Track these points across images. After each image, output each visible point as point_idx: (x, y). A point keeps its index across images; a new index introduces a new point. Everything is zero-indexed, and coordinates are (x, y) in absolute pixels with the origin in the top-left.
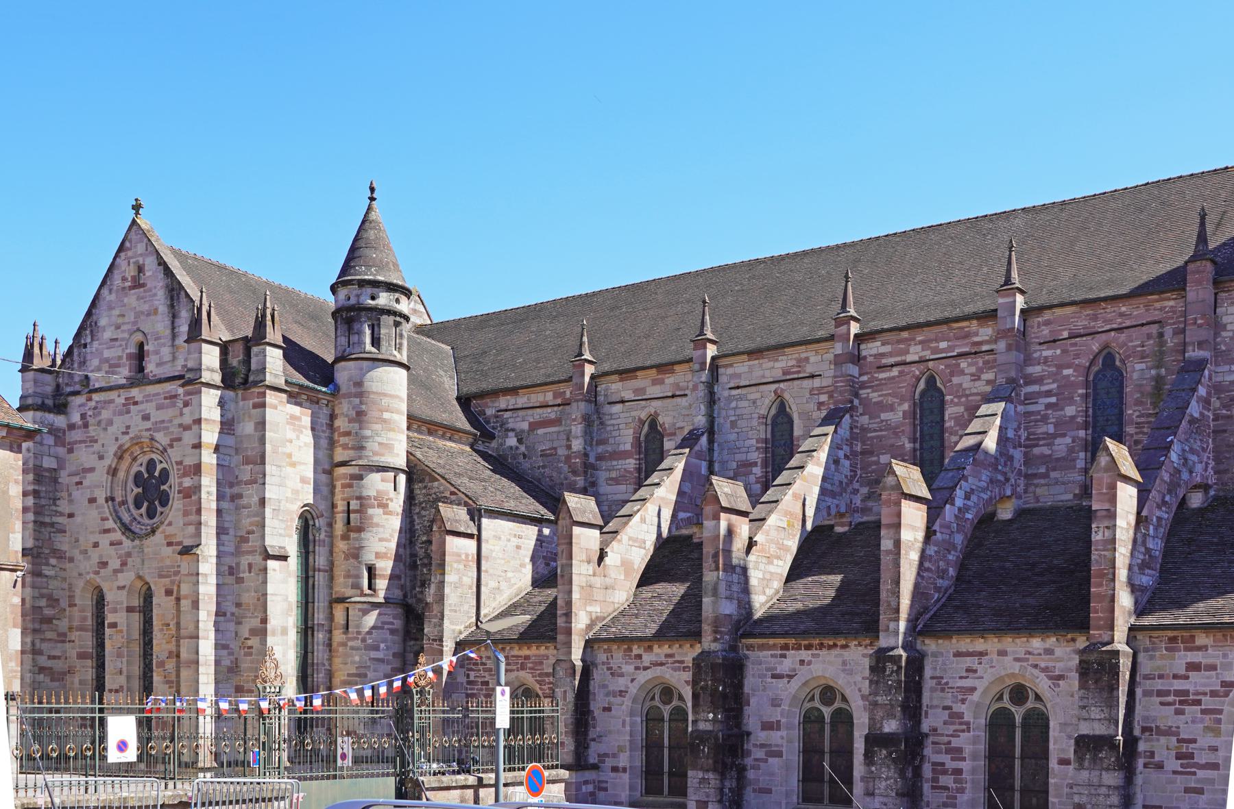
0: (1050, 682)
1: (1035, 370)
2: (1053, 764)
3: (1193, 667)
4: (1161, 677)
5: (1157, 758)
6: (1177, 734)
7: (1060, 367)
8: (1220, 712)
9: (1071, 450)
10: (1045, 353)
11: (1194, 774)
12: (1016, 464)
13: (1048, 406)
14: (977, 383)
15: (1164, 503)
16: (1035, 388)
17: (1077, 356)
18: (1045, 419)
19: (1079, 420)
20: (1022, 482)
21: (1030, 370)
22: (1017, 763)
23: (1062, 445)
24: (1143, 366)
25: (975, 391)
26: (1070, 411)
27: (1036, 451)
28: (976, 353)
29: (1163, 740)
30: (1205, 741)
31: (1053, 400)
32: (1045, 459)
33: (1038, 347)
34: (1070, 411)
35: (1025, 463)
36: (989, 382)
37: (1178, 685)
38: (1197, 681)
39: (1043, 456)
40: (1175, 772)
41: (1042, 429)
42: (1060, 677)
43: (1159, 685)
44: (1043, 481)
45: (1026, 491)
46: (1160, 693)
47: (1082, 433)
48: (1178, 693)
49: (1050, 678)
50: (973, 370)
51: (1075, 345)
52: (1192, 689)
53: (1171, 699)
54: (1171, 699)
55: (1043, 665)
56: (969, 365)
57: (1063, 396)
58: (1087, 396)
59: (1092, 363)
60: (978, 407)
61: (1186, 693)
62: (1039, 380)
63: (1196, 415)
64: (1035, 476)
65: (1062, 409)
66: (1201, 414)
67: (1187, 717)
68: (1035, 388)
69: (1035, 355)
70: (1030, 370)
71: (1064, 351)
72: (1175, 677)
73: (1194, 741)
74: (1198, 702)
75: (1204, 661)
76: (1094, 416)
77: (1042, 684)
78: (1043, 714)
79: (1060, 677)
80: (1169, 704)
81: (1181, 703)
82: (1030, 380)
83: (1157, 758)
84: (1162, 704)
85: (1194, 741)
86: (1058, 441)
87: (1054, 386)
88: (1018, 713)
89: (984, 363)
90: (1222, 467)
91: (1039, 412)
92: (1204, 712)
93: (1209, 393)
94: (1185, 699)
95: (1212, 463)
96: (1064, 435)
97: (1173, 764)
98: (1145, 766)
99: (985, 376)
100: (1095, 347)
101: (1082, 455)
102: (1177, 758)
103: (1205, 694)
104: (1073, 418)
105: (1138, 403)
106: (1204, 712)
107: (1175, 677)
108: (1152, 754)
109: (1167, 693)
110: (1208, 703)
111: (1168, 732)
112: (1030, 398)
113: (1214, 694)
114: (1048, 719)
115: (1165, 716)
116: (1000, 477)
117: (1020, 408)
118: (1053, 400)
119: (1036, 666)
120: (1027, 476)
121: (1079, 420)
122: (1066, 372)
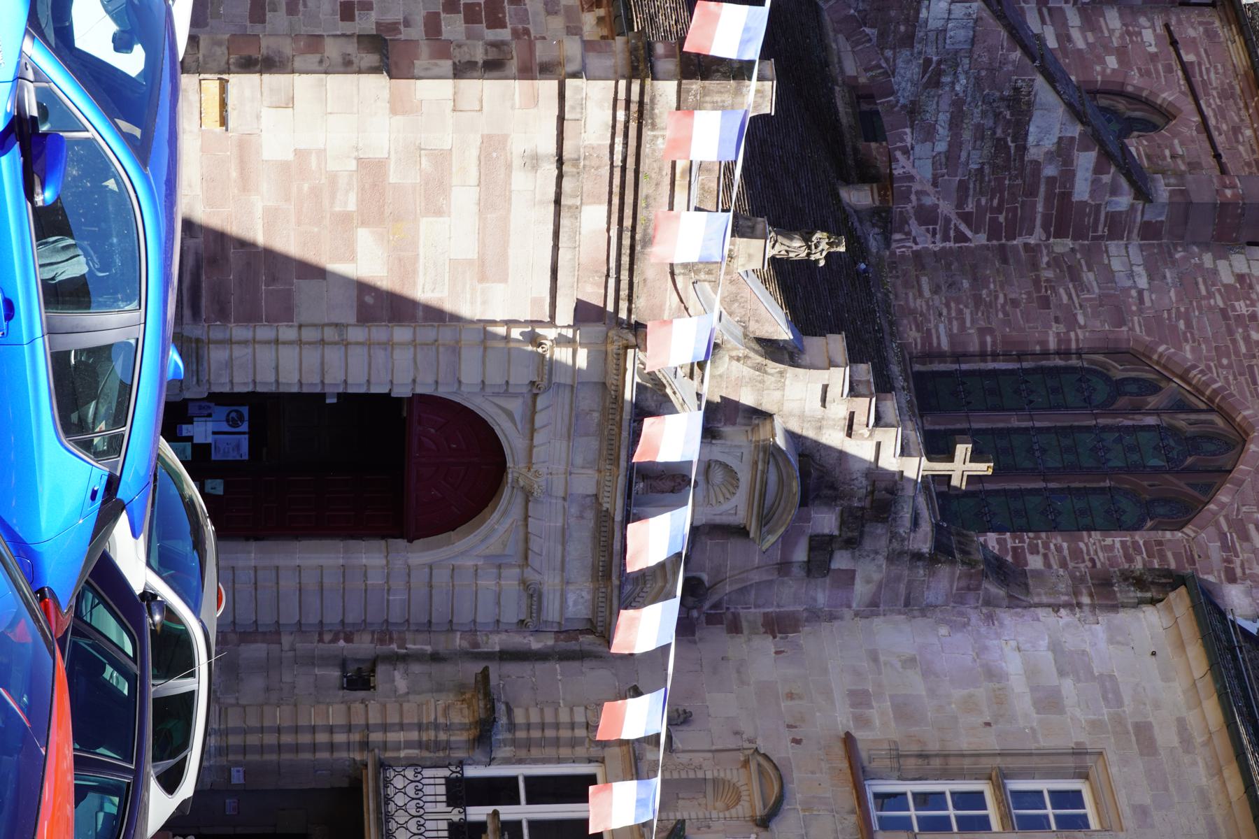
7: (1121, 53)
59: (1135, 98)
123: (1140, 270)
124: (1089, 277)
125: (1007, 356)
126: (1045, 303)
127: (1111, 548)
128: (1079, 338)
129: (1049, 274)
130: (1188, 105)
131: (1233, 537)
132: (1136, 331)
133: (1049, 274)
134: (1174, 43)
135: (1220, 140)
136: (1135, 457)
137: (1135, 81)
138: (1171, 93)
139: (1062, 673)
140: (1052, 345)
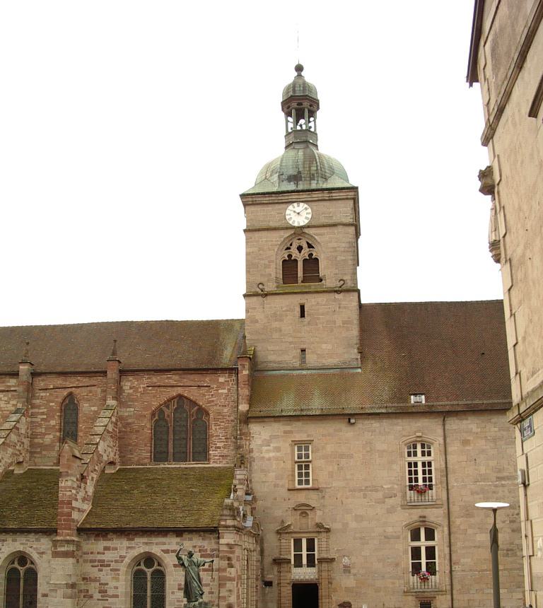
0: (38, 556)
1: (37, 402)
2: (39, 596)
3: (106, 548)
4: (92, 553)
5: (90, 593)
6: (99, 581)
8: (118, 570)
9: (53, 441)
10: (42, 394)
11: (107, 600)
12: (26, 447)
13: (42, 419)
14: (8, 405)
15: (95, 470)
16: (36, 410)
17: (57, 397)
18: (40, 425)
19: (57, 427)
20: (28, 455)
21: (34, 401)
22: (21, 597)
23: (48, 439)
24: (87, 405)
25: (6, 409)
26: (53, 423)
27: (36, 441)
28: (7, 391)
29: (93, 584)
30: (112, 584)
31: (45, 417)
32: (40, 445)
33: (37, 391)
34: (53, 423)
35: (30, 446)
36: (13, 405)
37: (99, 557)
38: (108, 556)
39: (39, 443)
40: (98, 600)
41: (39, 430)
42: (43, 553)
43: (91, 557)
44: (38, 456)
45: (30, 460)
46: (92, 561)
47: (58, 434)
48: (99, 561)
49: (38, 553)
50: (6, 399)
51: (56, 392)
52: (106, 559)
53: (96, 564)
54: (96, 564)
55: (35, 546)
56: (4, 396)
57: (50, 416)
58: (61, 416)
59: (64, 400)
60: (8, 417)
61: (104, 561)
62: (39, 407)
63: (111, 430)
64: (35, 452)
65: (49, 422)
66: (113, 430)
67: (104, 573)
68: (36, 410)
69: (38, 395)
70: (34, 401)
71: (50, 394)
72: (98, 553)
73: (107, 584)
74: (109, 566)
75: (112, 546)
76: (64, 426)
77: (35, 556)
78: (35, 571)
79: (43, 553)
80: (96, 566)
81: (101, 566)
82: (33, 406)
83: (90, 593)
84: (93, 566)
85: (107, 584)
86: (46, 437)
87: (46, 410)
88: (22, 570)
89: (12, 395)
90: (122, 454)
91: (38, 422)
92: (111, 570)
93: (116, 420)
94: (103, 564)
95: (118, 453)
96: (50, 434)
97: (97, 596)
98: (84, 597)
99: (11, 402)
100: (65, 394)
101: (58, 444)
102: (99, 592)
103: (112, 562)
104: (54, 426)
105: (84, 422)
106: (111, 570)
107: (98, 553)
108: (88, 591)
109: (95, 561)
110: (113, 565)
111: (95, 580)
112: (33, 415)
113: (116, 561)
114: (37, 574)
115: (94, 572)
116: (18, 453)
117: (29, 419)
118: (45, 417)
119: (31, 547)
120: (31, 452)
121: (57, 427)
122: (51, 404)
123: (128, 409)
124: (130, 421)
125: (151, 441)
126: (138, 431)
127: (216, 429)
128: (148, 426)
129: (128, 429)
130: (70, 390)
131: (212, 404)
132: (148, 413)
133: (128, 429)
134: (46, 389)
135: (81, 385)
136: (183, 419)
137: (60, 400)
138: (65, 393)
139: (269, 446)
140: (150, 431)
